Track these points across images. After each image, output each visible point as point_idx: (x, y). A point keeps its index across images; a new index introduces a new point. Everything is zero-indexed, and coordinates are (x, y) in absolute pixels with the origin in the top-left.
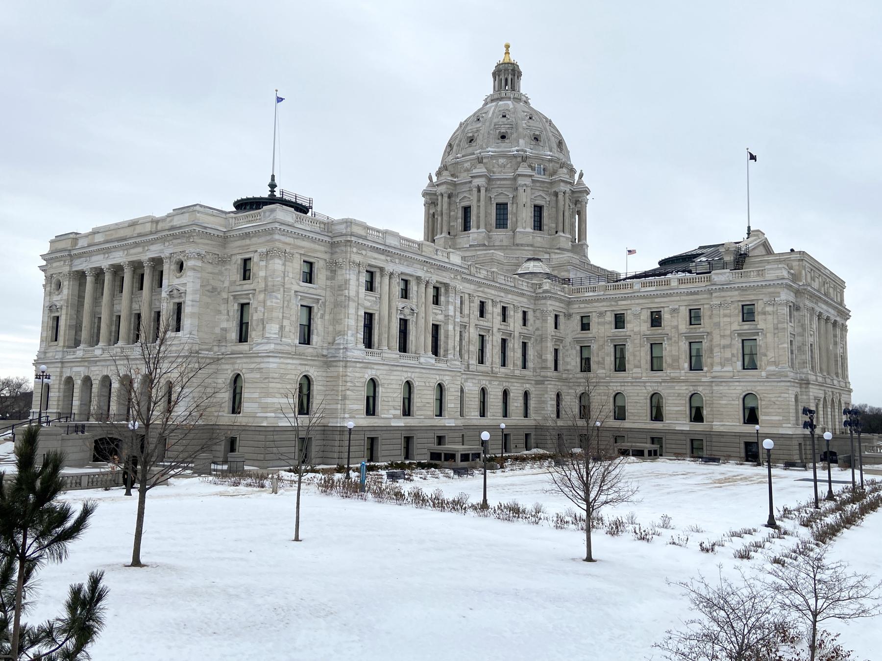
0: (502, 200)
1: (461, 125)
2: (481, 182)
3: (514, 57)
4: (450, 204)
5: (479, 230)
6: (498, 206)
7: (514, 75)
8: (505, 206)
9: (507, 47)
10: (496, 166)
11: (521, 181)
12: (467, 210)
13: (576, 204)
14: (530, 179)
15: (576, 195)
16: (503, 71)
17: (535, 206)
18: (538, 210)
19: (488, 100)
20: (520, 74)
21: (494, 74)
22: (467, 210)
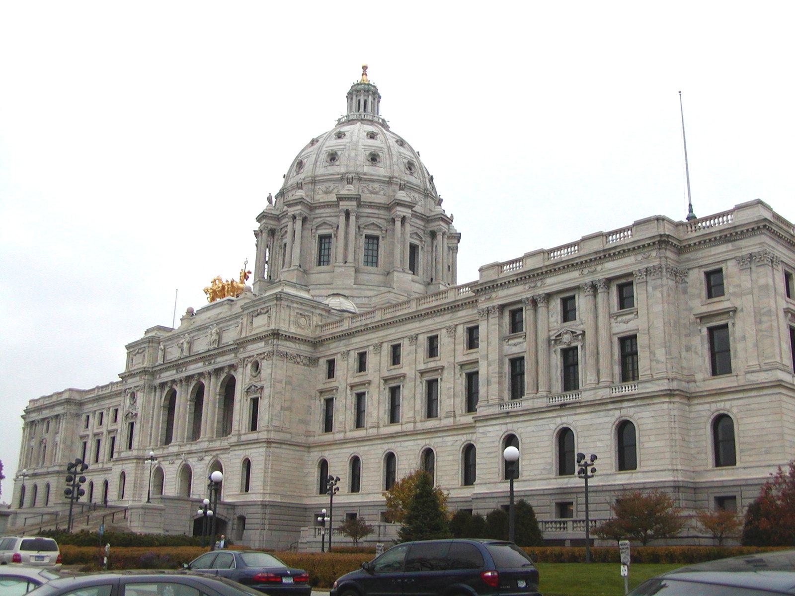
1: (313, 142)
2: (351, 205)
7: (374, 99)
9: (365, 68)
10: (366, 191)
12: (324, 239)
16: (362, 91)
18: (413, 249)
20: (380, 97)
21: (350, 96)
22: (324, 239)
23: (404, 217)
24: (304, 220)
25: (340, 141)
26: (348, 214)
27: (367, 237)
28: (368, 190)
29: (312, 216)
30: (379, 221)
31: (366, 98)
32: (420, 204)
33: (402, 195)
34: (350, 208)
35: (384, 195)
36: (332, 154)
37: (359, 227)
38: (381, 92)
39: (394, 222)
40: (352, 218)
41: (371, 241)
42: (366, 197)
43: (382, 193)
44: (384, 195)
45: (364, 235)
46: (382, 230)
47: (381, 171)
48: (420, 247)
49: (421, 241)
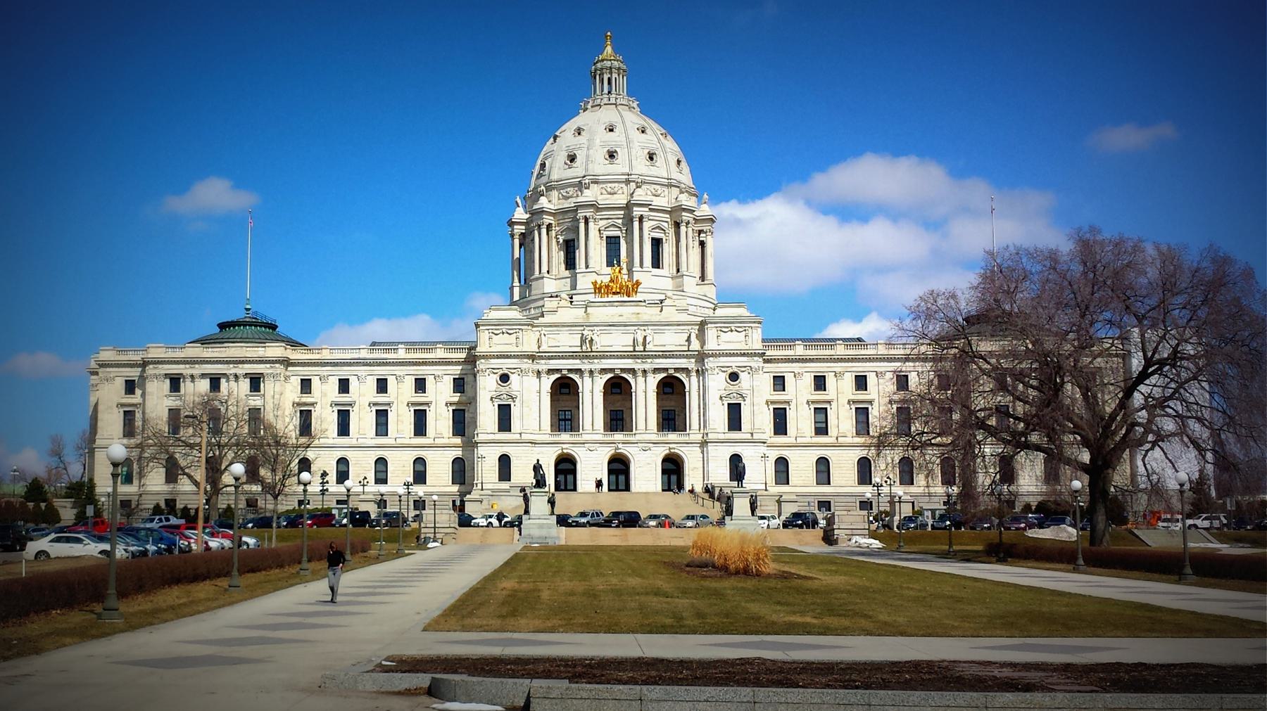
8: (617, 239)
10: (604, 192)
11: (637, 212)
18: (657, 243)
23: (642, 215)
24: (549, 227)
25: (580, 137)
28: (607, 191)
33: (641, 195)
34: (588, 215)
37: (599, 230)
39: (633, 223)
40: (591, 224)
42: (604, 200)
43: (620, 192)
45: (605, 238)
46: (621, 231)
47: (620, 167)
48: (664, 240)
49: (665, 233)
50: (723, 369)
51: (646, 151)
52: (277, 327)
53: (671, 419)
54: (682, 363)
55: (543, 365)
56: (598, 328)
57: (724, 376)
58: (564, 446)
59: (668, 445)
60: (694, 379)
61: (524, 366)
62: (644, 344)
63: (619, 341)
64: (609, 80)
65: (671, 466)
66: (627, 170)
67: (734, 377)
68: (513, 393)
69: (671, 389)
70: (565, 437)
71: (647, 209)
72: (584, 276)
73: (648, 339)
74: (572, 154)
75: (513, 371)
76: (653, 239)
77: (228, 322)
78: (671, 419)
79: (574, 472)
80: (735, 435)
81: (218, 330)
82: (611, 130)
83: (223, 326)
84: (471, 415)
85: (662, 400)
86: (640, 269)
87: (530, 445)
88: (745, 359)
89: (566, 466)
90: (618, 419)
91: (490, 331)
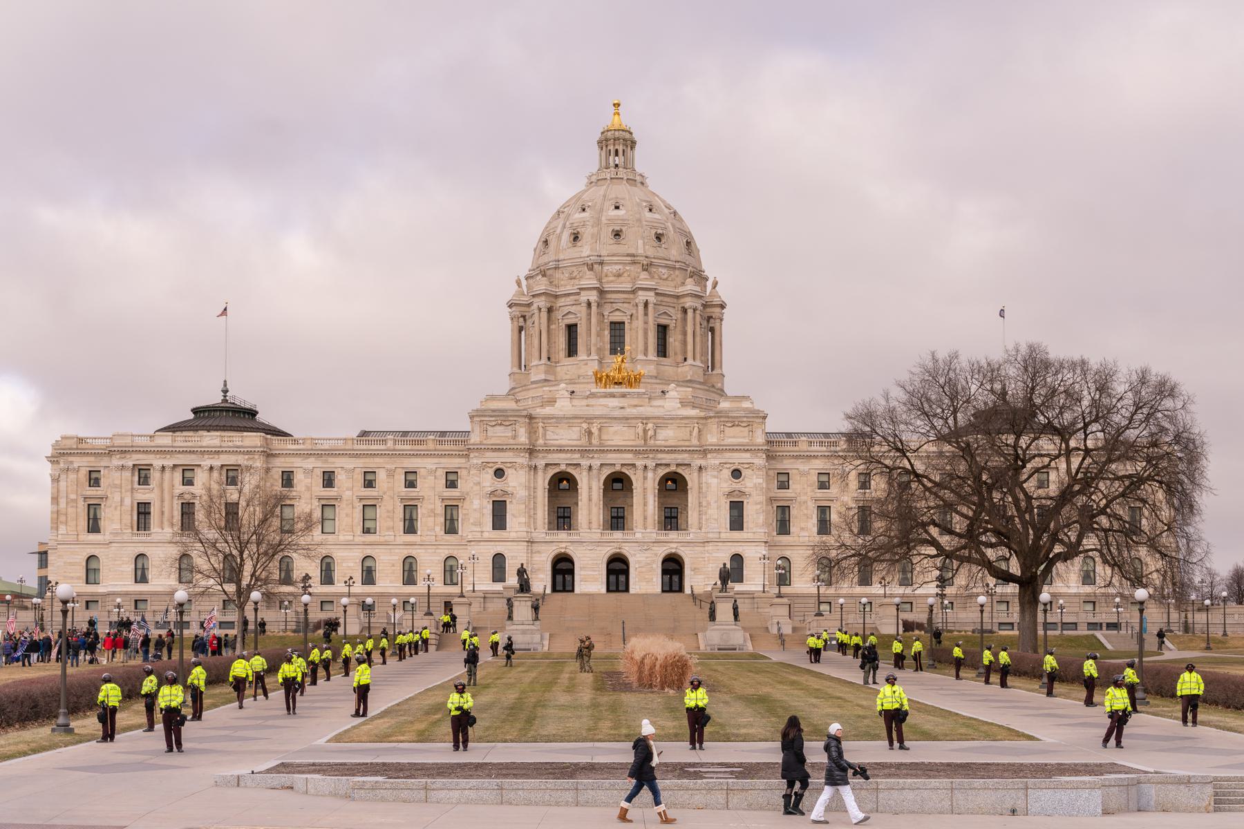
0: (617, 317)
3: (627, 119)
4: (549, 319)
5: (590, 358)
6: (613, 325)
9: (617, 105)
12: (572, 329)
13: (708, 321)
14: (652, 294)
15: (708, 310)
17: (658, 325)
18: (663, 330)
19: (594, 179)
20: (633, 143)
21: (600, 142)
22: (572, 329)
24: (550, 310)
26: (589, 304)
27: (611, 323)
29: (558, 305)
30: (625, 305)
31: (617, 147)
32: (670, 279)
35: (629, 276)
36: (574, 234)
38: (636, 136)
40: (594, 308)
41: (617, 325)
43: (626, 275)
44: (629, 276)
50: (725, 466)
51: (653, 232)
52: (257, 413)
53: (671, 519)
54: (682, 458)
55: (541, 463)
56: (599, 421)
57: (727, 473)
58: (564, 545)
59: (669, 544)
60: (696, 474)
61: (519, 460)
62: (646, 440)
63: (618, 436)
64: (617, 151)
65: (672, 566)
66: (632, 251)
67: (736, 474)
68: (509, 489)
69: (673, 485)
70: (563, 535)
71: (652, 294)
72: (586, 364)
73: (650, 433)
74: (575, 232)
75: (509, 465)
76: (658, 325)
77: (201, 407)
78: (671, 519)
79: (571, 572)
80: (736, 535)
81: (192, 416)
82: (617, 208)
83: (196, 411)
84: (464, 512)
85: (665, 497)
86: (645, 358)
87: (526, 543)
88: (748, 455)
89: (563, 568)
90: (617, 520)
91: (485, 422)
